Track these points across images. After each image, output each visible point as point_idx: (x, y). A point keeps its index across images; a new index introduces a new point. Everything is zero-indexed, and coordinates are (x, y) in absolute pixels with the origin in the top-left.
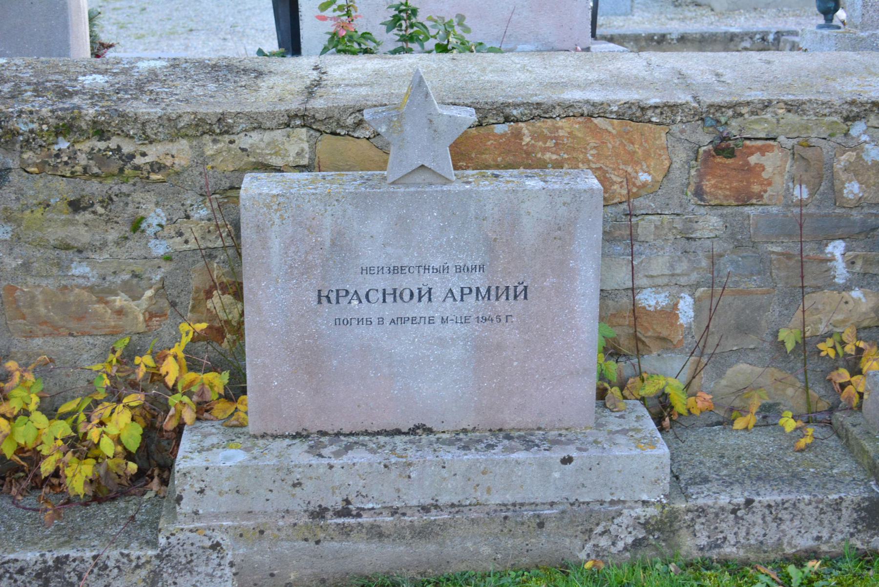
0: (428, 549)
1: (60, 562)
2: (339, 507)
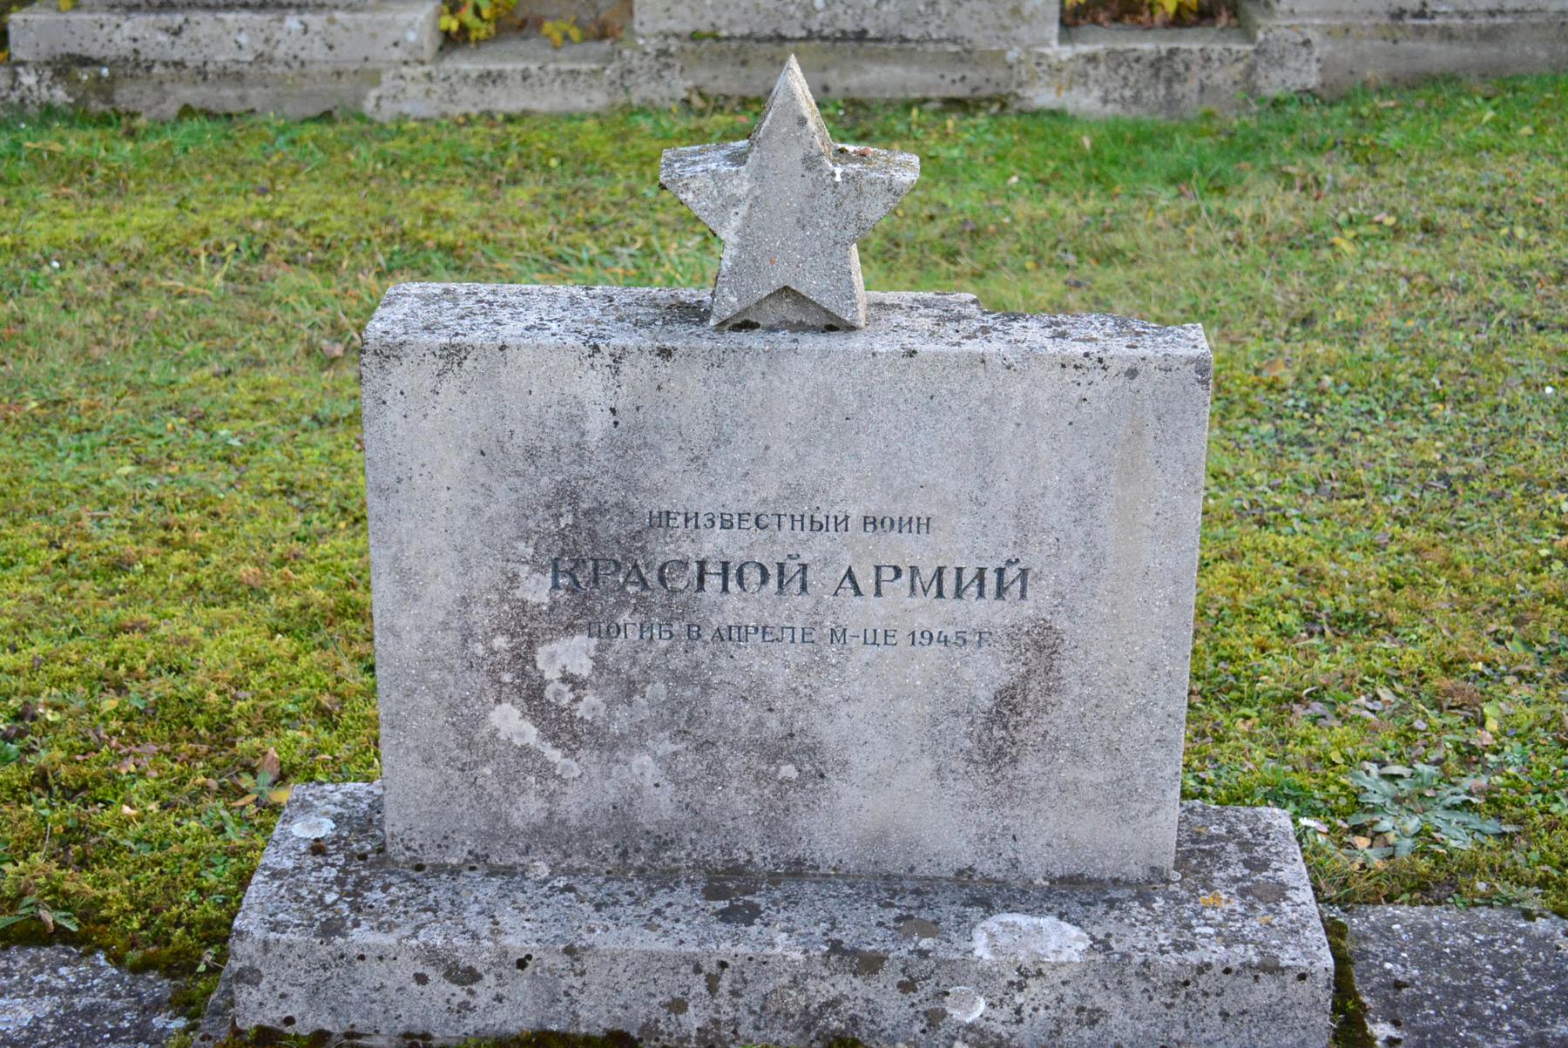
0: (1491, 51)
1: (1172, 53)
2: (1417, 8)
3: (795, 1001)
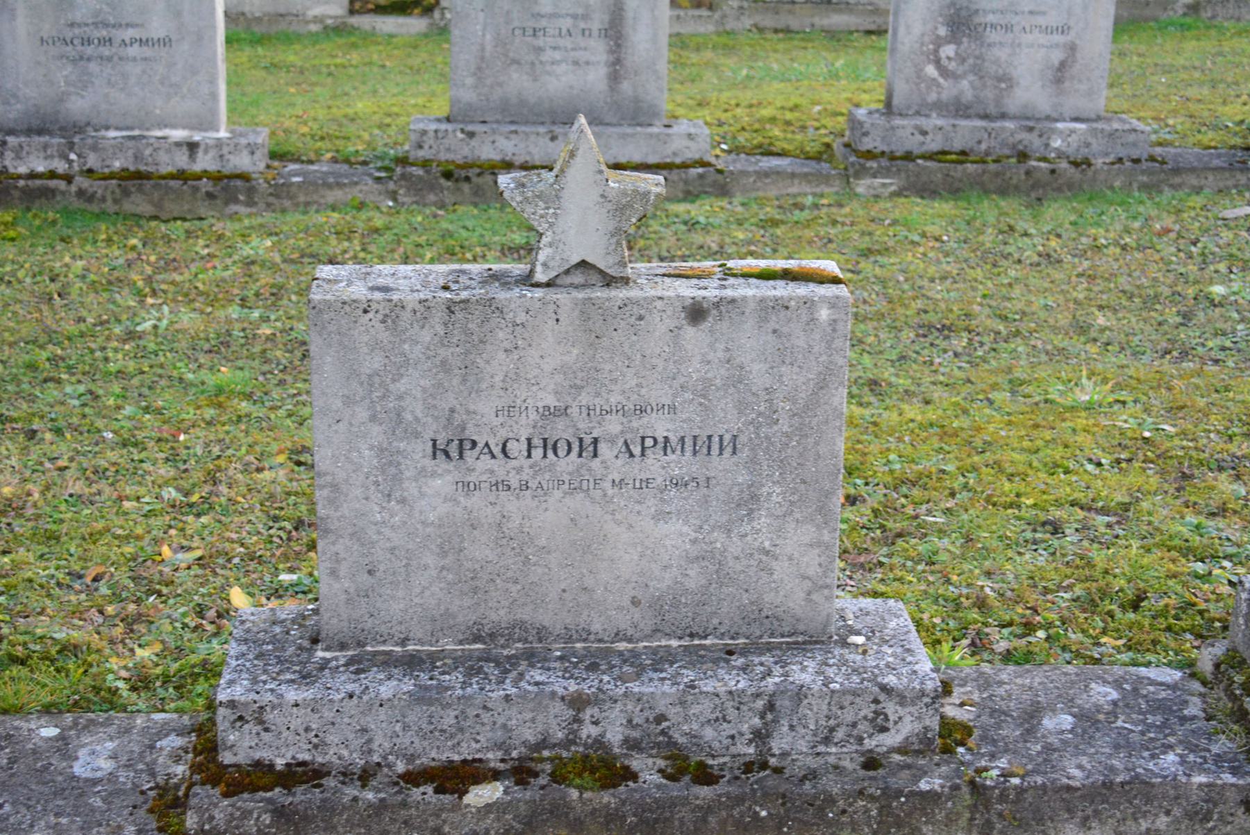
3: (1011, 140)
